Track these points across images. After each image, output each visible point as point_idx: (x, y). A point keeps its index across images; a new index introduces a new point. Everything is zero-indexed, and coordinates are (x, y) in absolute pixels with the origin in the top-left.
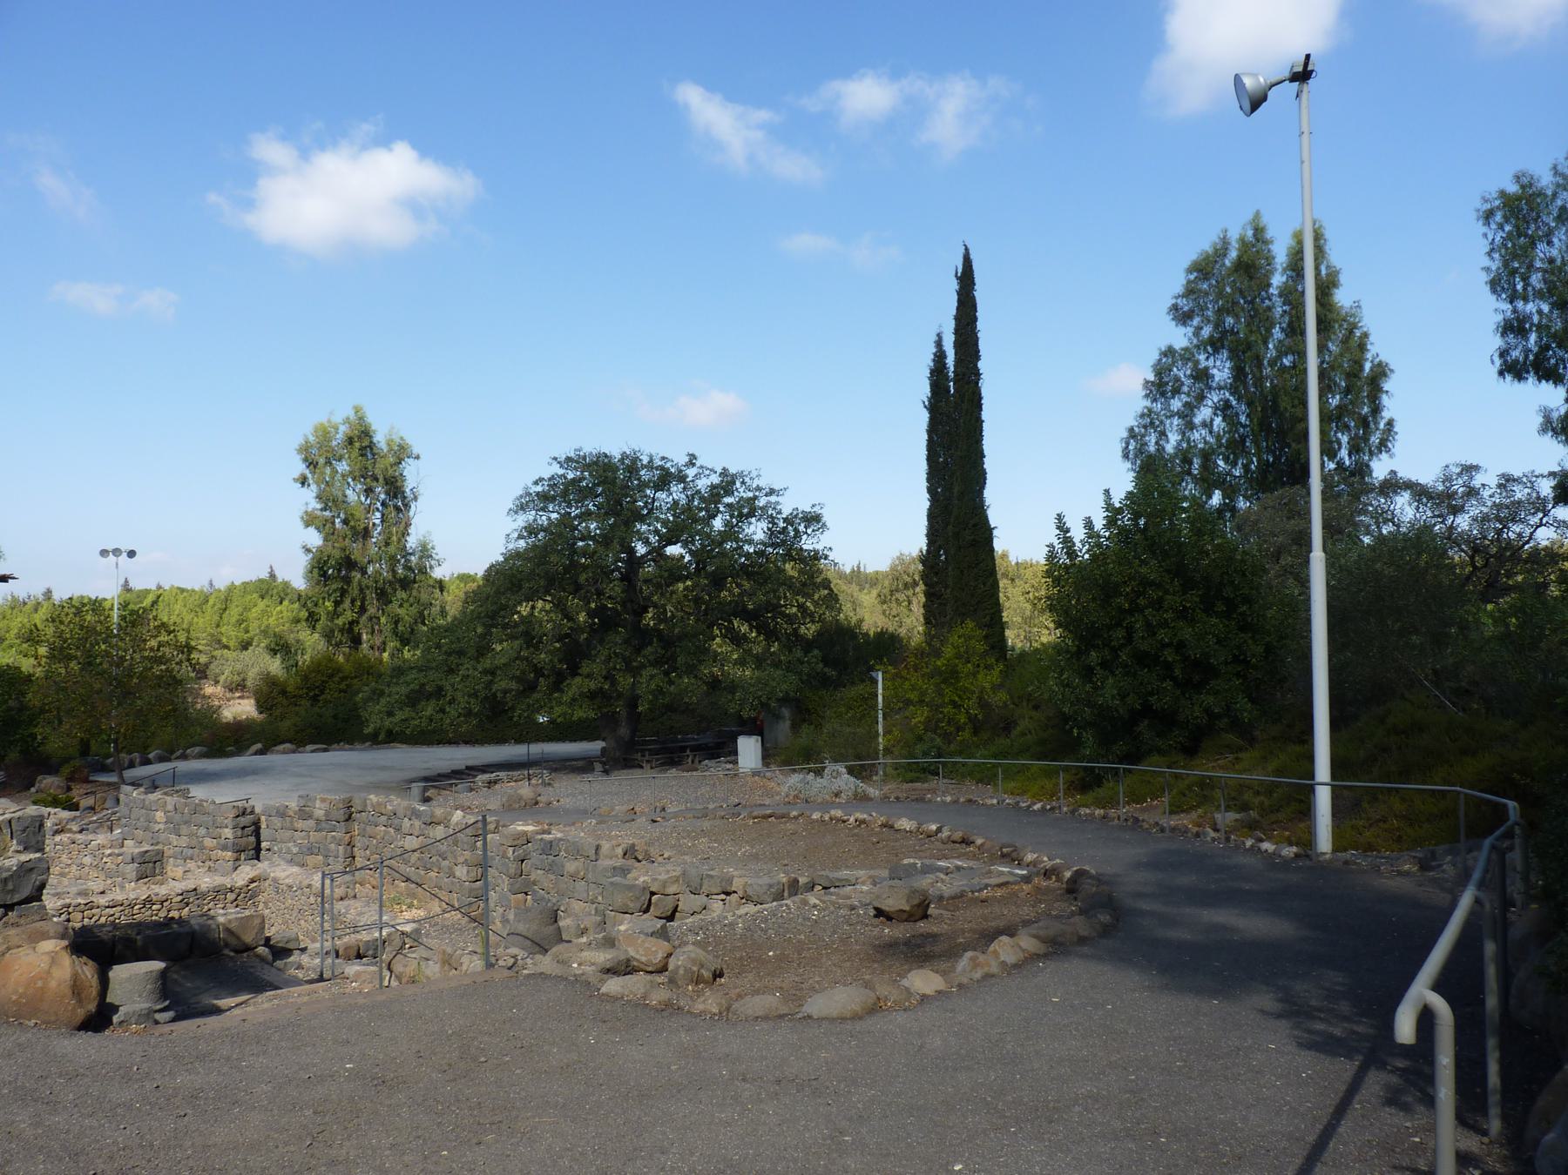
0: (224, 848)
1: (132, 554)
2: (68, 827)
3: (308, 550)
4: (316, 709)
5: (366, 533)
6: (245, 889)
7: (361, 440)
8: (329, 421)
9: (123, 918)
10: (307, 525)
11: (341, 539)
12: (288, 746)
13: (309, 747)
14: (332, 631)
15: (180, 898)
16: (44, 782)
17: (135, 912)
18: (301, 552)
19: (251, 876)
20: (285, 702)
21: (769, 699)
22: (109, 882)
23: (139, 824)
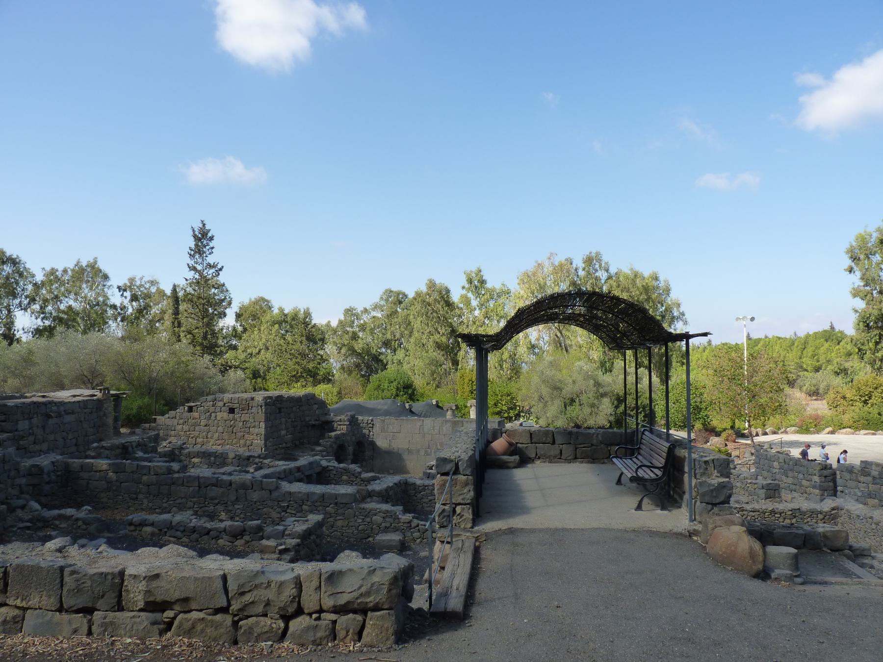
0: (814, 487)
1: (752, 319)
3: (856, 311)
4: (866, 408)
6: (829, 513)
8: (865, 232)
9: (759, 519)
10: (855, 296)
11: (878, 303)
12: (848, 429)
14: (875, 361)
15: (791, 512)
20: (846, 404)
22: (750, 497)
23: (764, 468)
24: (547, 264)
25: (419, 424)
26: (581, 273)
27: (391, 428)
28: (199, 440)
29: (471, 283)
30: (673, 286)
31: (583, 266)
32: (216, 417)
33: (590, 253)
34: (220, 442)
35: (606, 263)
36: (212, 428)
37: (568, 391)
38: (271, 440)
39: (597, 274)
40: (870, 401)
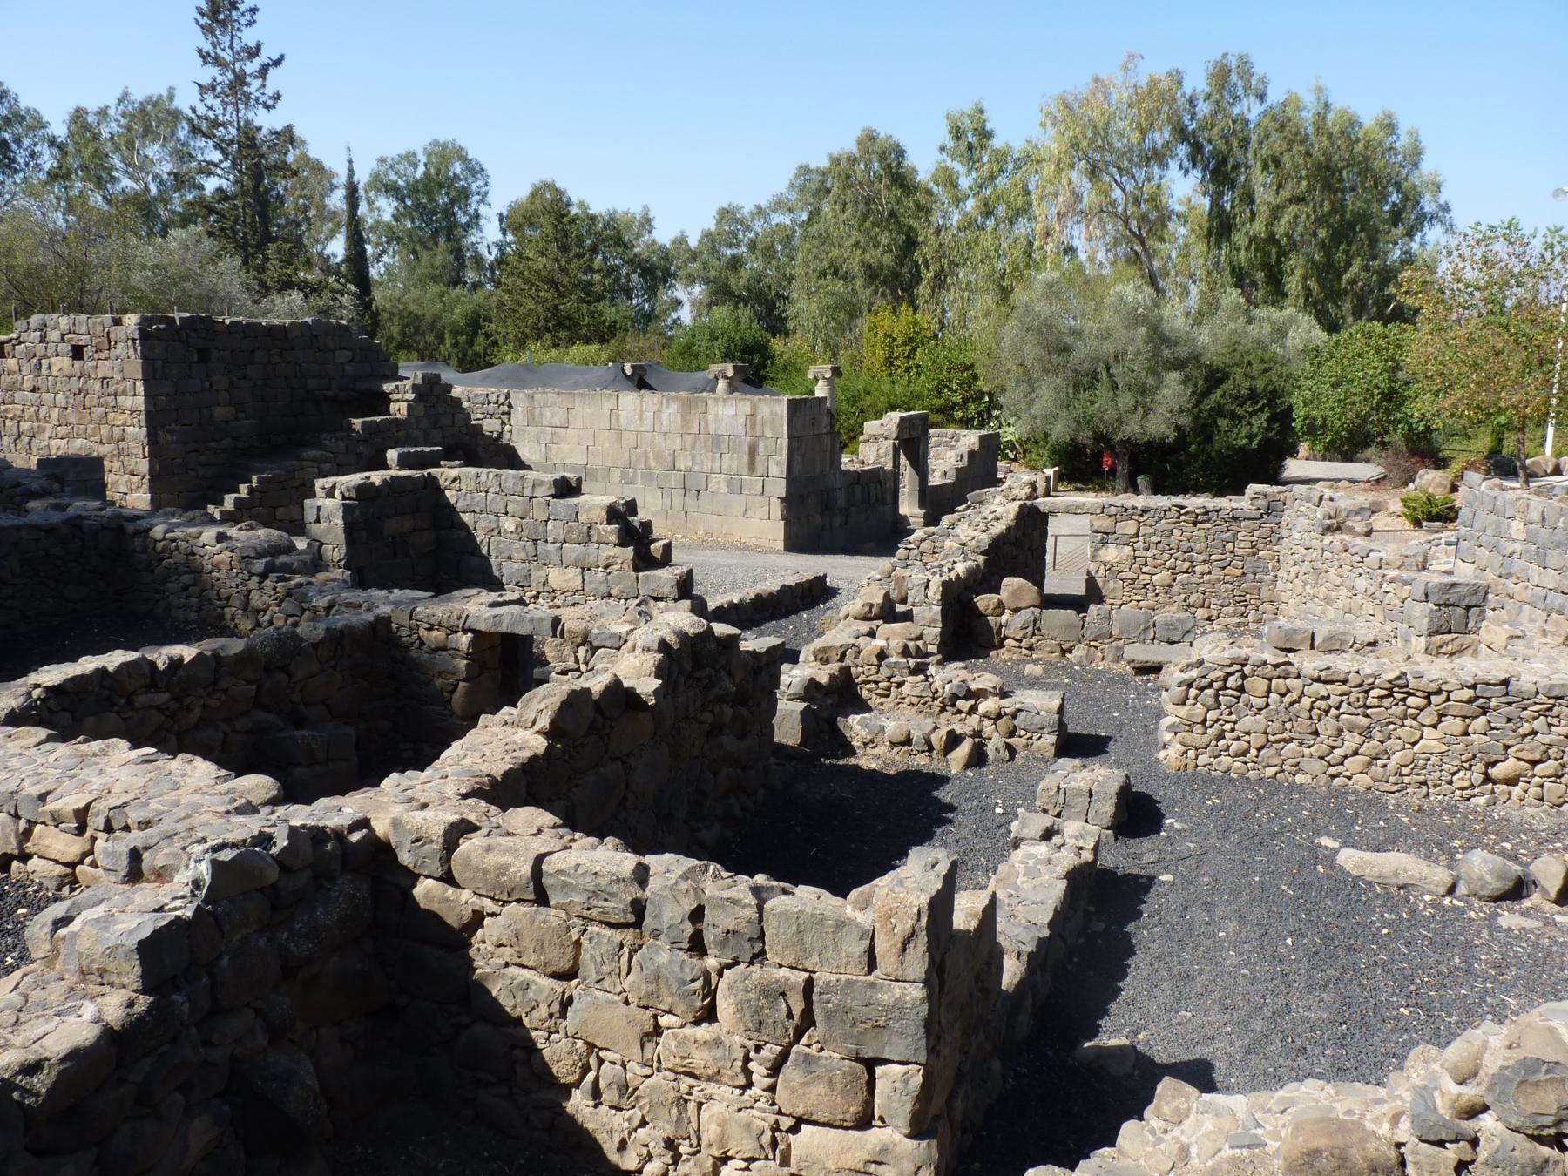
2: (1349, 523)
9: (1344, 707)
15: (1467, 694)
16: (1426, 477)
17: (1370, 701)
23: (1483, 540)
24: (1119, 79)
25: (609, 404)
26: (1204, 108)
27: (549, 415)
28: (25, 426)
29: (958, 138)
30: (1426, 142)
31: (1208, 89)
32: (49, 368)
33: (1225, 56)
34: (62, 430)
35: (1262, 79)
36: (48, 397)
37: (1083, 351)
38: (173, 426)
39: (1236, 110)
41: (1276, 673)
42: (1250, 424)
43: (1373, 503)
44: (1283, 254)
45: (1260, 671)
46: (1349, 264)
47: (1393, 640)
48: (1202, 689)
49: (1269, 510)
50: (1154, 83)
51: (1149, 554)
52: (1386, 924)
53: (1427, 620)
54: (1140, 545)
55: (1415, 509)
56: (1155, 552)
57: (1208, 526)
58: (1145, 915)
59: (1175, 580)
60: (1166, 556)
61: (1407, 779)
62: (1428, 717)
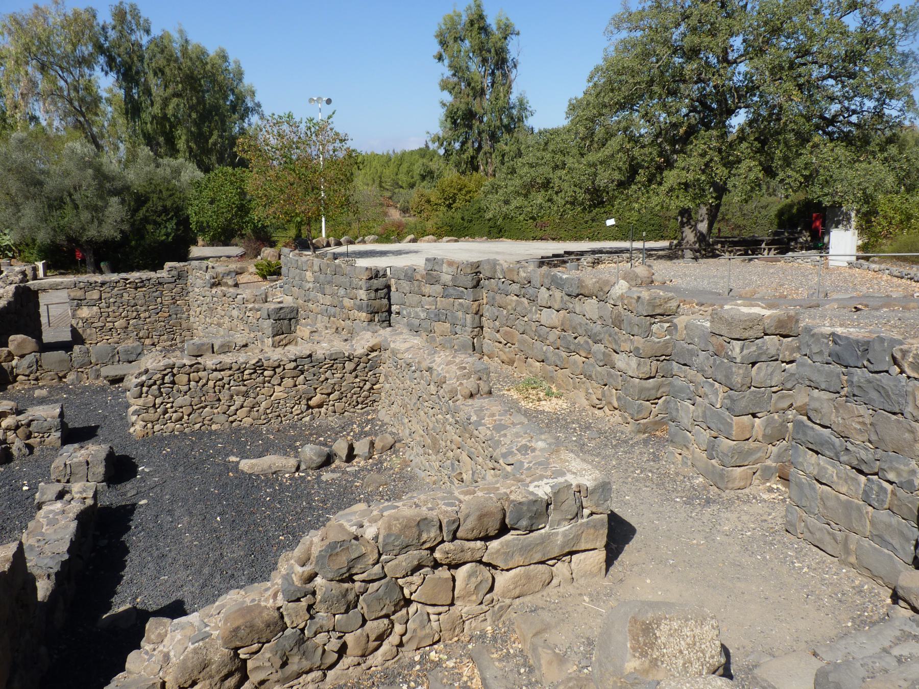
0: (360, 309)
1: (329, 101)
2: (224, 280)
3: (444, 105)
5: (482, 92)
6: (364, 359)
7: (478, 24)
8: (455, 11)
9: (232, 382)
12: (431, 237)
13: (446, 239)
15: (293, 364)
17: (245, 377)
18: (439, 105)
19: (370, 344)
20: (430, 208)
21: (875, 190)
23: (295, 283)
26: (112, 34)
30: (244, 68)
31: (113, 23)
33: (121, 3)
35: (146, 21)
37: (50, 185)
39: (133, 38)
40: (454, 205)
41: (192, 370)
42: (166, 227)
43: (241, 268)
44: (172, 126)
45: (182, 370)
46: (211, 134)
47: (256, 342)
48: (150, 387)
49: (179, 277)
50: (77, 15)
51: (110, 310)
52: (268, 495)
53: (271, 329)
54: (103, 305)
55: (262, 270)
56: (113, 308)
57: (144, 289)
58: (133, 527)
59: (129, 324)
60: (121, 310)
61: (270, 416)
62: (275, 381)
